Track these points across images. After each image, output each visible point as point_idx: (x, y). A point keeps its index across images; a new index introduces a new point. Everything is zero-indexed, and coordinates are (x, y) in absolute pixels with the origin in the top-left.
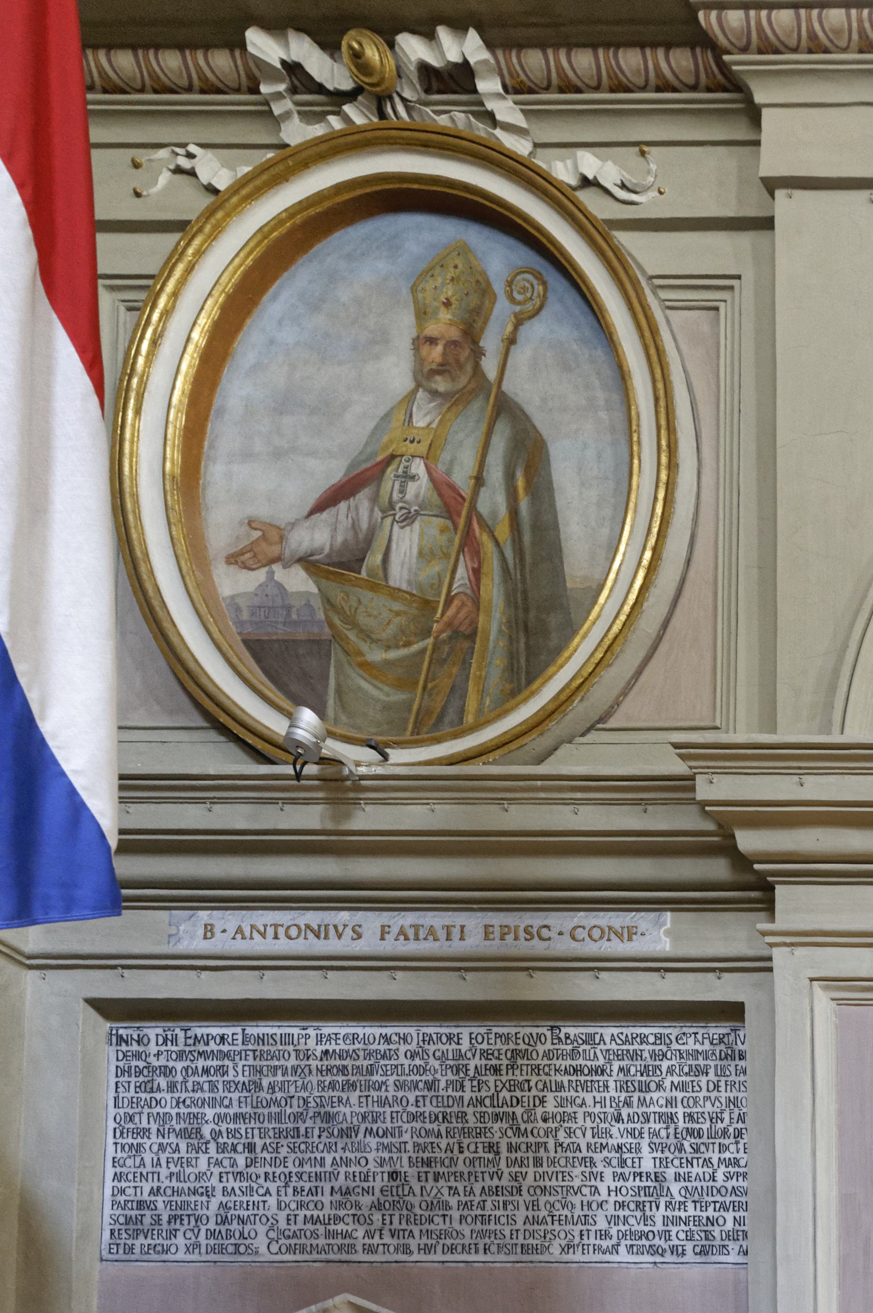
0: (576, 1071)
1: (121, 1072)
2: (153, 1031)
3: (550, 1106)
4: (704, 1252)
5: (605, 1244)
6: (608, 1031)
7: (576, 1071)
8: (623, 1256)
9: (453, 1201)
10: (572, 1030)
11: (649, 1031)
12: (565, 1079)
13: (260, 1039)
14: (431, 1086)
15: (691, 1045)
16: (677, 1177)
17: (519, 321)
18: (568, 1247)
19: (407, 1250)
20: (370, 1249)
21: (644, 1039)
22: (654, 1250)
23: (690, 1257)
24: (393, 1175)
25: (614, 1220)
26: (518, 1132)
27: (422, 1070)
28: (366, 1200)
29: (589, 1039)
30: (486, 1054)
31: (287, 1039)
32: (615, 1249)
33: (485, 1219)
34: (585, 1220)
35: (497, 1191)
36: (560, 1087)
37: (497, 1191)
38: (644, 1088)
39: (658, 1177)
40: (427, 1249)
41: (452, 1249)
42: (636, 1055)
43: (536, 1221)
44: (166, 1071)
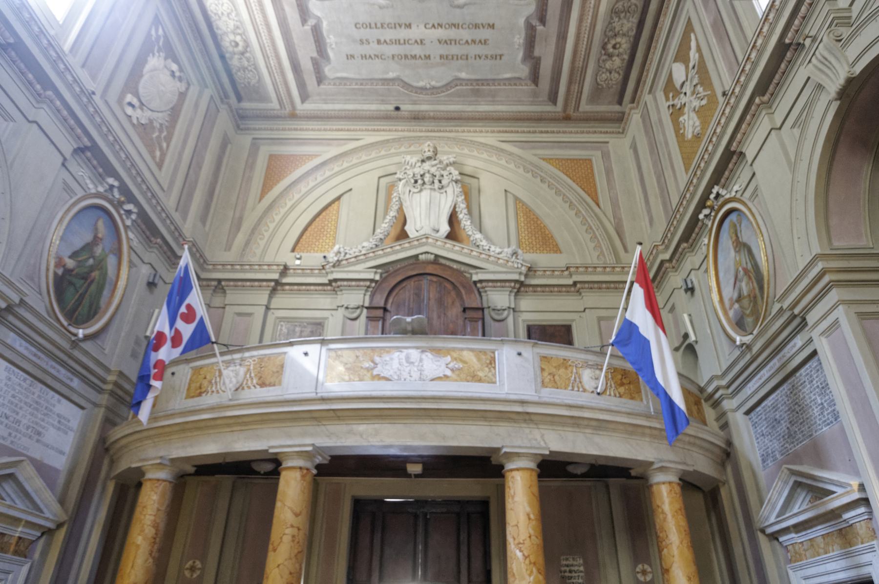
0: (802, 384)
1: (753, 425)
2: (752, 414)
3: (801, 396)
4: (836, 420)
5: (820, 427)
6: (802, 371)
7: (802, 384)
8: (825, 429)
9: (797, 430)
10: (798, 374)
11: (807, 366)
12: (800, 388)
13: (764, 407)
14: (785, 403)
15: (815, 364)
16: (825, 401)
17: (740, 226)
18: (816, 432)
19: (795, 446)
20: (791, 449)
21: (807, 369)
22: (828, 424)
23: (834, 423)
24: (788, 428)
25: (820, 419)
26: (800, 406)
27: (783, 400)
28: (786, 437)
29: (801, 375)
30: (789, 389)
31: (766, 405)
32: (822, 428)
33: (802, 432)
34: (816, 423)
35: (801, 423)
36: (801, 390)
37: (801, 423)
38: (812, 381)
39: (822, 404)
40: (798, 444)
41: (801, 442)
42: (808, 374)
43: (809, 428)
44: (756, 422)
